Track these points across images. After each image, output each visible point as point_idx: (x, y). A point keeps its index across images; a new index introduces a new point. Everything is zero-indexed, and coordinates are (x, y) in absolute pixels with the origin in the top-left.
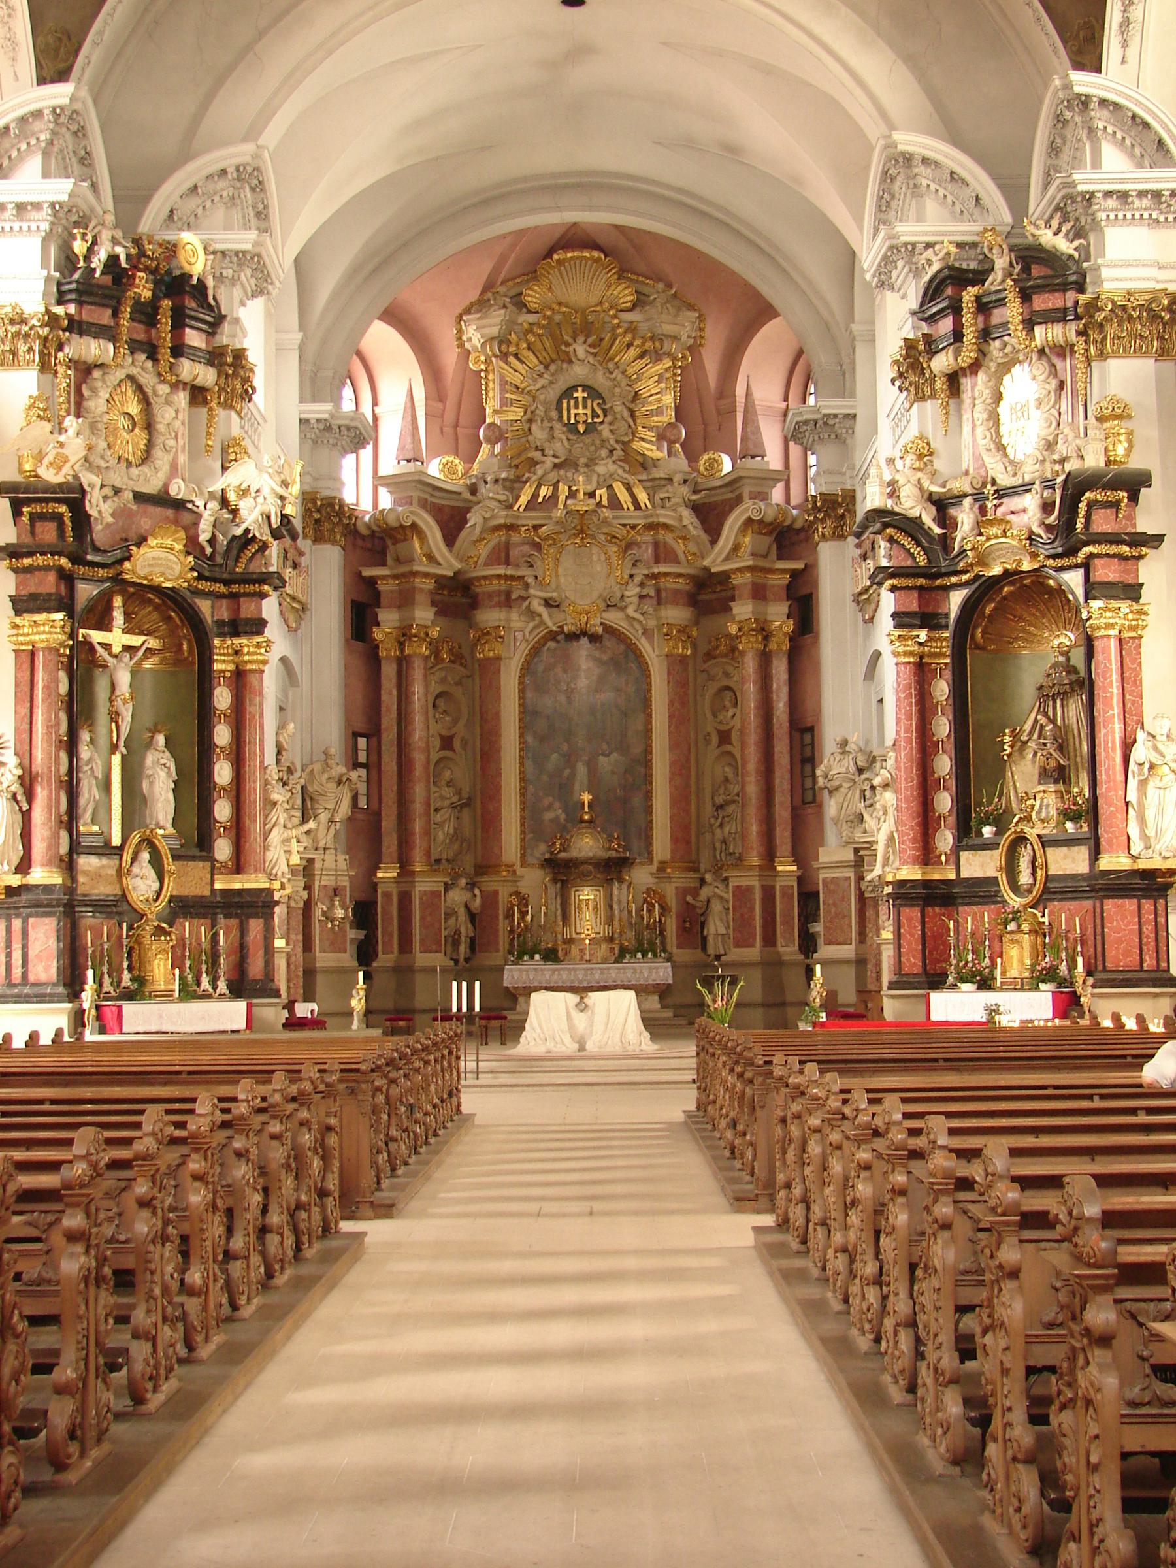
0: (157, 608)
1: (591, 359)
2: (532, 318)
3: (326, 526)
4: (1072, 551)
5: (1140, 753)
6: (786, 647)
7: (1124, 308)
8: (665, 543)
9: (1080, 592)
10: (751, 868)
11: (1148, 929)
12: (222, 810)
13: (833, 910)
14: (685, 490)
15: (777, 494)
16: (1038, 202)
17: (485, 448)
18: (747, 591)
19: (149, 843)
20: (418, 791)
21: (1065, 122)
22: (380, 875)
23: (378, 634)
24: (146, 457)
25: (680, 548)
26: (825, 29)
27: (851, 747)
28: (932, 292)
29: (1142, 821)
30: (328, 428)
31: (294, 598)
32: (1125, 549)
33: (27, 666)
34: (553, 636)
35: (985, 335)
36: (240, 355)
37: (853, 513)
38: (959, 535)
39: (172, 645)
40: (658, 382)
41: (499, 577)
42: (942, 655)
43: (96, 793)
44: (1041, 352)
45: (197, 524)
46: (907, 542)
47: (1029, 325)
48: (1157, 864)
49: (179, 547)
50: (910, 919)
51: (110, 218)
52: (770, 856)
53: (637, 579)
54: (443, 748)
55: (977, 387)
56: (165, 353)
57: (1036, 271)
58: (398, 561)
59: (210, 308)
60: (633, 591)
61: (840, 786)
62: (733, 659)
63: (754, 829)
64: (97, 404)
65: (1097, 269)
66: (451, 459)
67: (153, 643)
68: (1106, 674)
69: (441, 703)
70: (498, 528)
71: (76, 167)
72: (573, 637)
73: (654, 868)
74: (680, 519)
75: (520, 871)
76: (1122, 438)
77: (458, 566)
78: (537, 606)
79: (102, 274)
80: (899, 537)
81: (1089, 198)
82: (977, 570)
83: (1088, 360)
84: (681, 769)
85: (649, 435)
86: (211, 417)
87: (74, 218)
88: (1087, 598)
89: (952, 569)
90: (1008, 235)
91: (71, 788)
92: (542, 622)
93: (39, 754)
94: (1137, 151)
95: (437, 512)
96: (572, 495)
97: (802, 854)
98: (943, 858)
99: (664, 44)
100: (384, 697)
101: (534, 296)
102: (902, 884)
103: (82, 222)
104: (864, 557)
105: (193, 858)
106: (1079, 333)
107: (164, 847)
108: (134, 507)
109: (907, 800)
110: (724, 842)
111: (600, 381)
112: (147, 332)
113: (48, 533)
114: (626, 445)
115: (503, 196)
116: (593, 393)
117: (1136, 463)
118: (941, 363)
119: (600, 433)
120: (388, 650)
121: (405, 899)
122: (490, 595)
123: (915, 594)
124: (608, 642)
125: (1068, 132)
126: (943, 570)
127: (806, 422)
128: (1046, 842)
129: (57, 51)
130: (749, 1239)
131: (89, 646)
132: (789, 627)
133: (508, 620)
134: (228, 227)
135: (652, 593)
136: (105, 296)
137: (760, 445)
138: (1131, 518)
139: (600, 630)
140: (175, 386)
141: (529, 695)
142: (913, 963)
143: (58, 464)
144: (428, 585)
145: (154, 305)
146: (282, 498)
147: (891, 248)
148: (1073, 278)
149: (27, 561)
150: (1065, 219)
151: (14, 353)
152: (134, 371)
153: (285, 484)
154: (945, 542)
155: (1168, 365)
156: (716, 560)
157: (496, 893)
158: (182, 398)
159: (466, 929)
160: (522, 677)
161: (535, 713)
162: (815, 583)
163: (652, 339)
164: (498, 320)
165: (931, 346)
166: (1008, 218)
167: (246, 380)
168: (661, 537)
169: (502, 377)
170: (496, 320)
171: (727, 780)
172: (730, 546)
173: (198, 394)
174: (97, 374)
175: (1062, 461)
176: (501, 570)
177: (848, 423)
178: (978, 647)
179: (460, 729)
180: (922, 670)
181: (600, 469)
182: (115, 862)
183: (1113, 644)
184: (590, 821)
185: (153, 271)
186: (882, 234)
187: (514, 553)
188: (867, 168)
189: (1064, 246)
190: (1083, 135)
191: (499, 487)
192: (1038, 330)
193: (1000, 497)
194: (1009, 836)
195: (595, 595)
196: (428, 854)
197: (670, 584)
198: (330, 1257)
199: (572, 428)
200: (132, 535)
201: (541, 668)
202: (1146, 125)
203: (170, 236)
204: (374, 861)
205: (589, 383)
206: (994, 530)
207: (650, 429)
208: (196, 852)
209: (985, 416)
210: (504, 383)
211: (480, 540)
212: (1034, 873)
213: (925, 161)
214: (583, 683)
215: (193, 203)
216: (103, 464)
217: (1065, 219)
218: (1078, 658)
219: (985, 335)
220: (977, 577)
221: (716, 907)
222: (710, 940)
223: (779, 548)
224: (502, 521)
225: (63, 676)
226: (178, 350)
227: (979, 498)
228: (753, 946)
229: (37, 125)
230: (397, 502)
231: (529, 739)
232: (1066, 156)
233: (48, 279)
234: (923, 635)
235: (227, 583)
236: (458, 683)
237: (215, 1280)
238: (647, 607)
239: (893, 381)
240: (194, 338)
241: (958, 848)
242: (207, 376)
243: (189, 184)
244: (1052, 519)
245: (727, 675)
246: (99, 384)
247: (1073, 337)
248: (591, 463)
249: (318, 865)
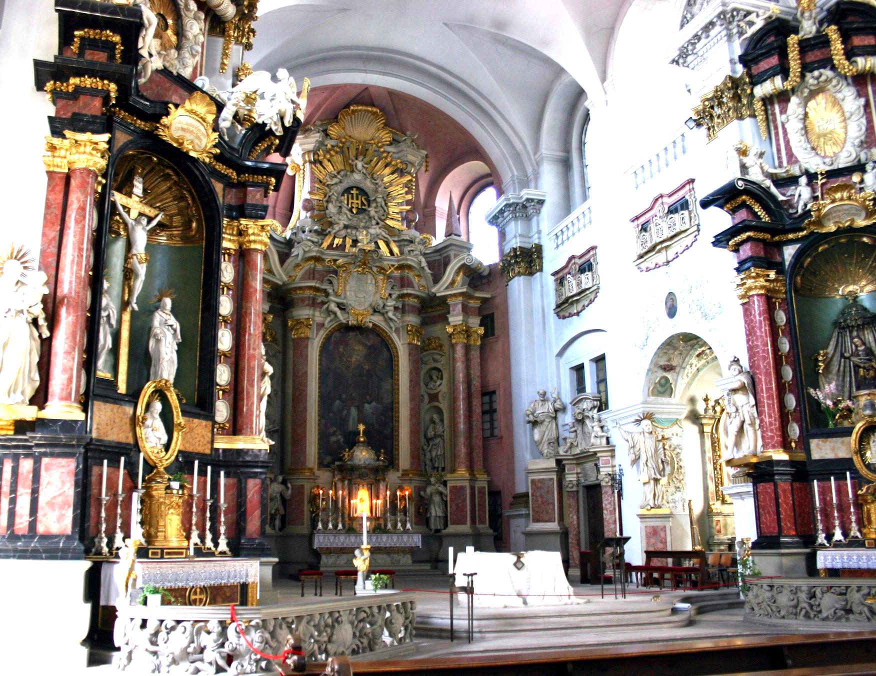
1: (364, 171)
6: (479, 343)
8: (408, 278)
13: (540, 499)
25: (416, 280)
53: (394, 296)
60: (391, 303)
61: (544, 421)
62: (441, 350)
84: (415, 414)
89: (795, 226)
111: (368, 185)
126: (787, 227)
132: (481, 331)
133: (314, 315)
135: (401, 307)
156: (440, 290)
168: (406, 274)
172: (450, 280)
181: (372, 231)
182: (129, 410)
195: (367, 305)
197: (413, 301)
207: (398, 213)
210: (314, 179)
228: (465, 523)
245: (435, 361)
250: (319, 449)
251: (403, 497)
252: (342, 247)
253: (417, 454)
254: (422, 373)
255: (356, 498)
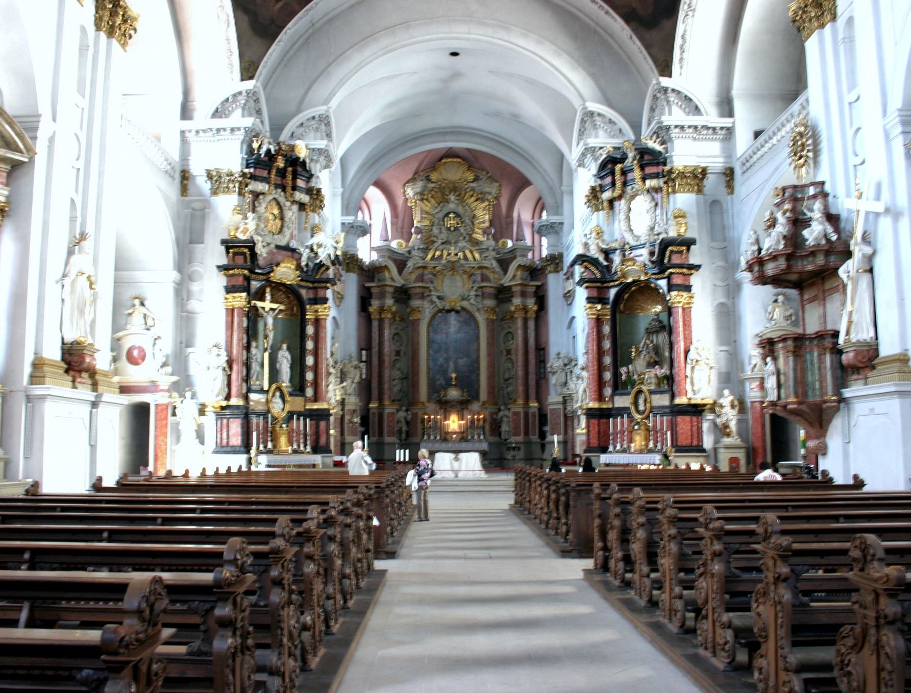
0: (284, 293)
2: (433, 185)
3: (351, 266)
4: (662, 272)
5: (692, 355)
6: (534, 316)
7: (683, 172)
9: (665, 288)
10: (519, 404)
11: (695, 428)
12: (309, 376)
14: (494, 253)
15: (530, 255)
16: (645, 132)
17: (414, 236)
18: (518, 294)
19: (279, 389)
20: (387, 372)
21: (657, 98)
22: (371, 405)
23: (371, 309)
24: (281, 231)
25: (491, 276)
26: (557, 62)
27: (562, 356)
28: (603, 166)
29: (692, 383)
30: (352, 227)
31: (339, 293)
32: (685, 271)
33: (230, 315)
34: (440, 311)
35: (625, 184)
36: (319, 191)
37: (561, 261)
38: (614, 266)
39: (290, 308)
40: (484, 210)
41: (419, 287)
42: (606, 315)
43: (258, 368)
44: (648, 191)
45: (300, 259)
46: (593, 269)
47: (644, 179)
48: (699, 402)
49: (293, 267)
50: (594, 424)
51: (268, 134)
52: (527, 399)
53: (475, 288)
54: (396, 355)
55: (621, 205)
56: (289, 189)
57: (646, 157)
58: (379, 280)
59: (307, 171)
60: (473, 293)
63: (521, 389)
64: (261, 209)
65: (671, 157)
66: (400, 240)
67: (282, 307)
68: (677, 322)
69: (396, 337)
70: (419, 267)
71: (255, 115)
72: (449, 311)
73: (480, 404)
74: (492, 264)
75: (427, 405)
76: (683, 225)
77: (403, 282)
78: (434, 299)
79: (265, 156)
80: (589, 266)
81: (668, 128)
82: (622, 280)
83: (668, 194)
84: (492, 365)
85: (480, 231)
86: (307, 215)
87: (253, 134)
88: (669, 290)
90: (633, 145)
91: (247, 365)
92: (436, 306)
93: (235, 351)
94: (687, 110)
95: (395, 261)
96: (449, 254)
97: (540, 398)
98: (607, 399)
99: (490, 72)
100: (373, 335)
101: (434, 176)
102: (591, 409)
103: (257, 136)
104: (568, 279)
105: (297, 395)
106: (665, 183)
107: (286, 391)
108: (275, 251)
109: (593, 375)
110: (508, 394)
111: (460, 210)
112: (282, 180)
113: (240, 260)
114: (470, 235)
115: (423, 136)
116: (457, 215)
117: (689, 235)
118: (607, 195)
119: (460, 230)
120: (375, 316)
121: (381, 415)
122: (416, 294)
123: (596, 290)
124: (463, 314)
125: (658, 102)
127: (543, 226)
128: (651, 392)
129: (249, 69)
130: (581, 575)
131: (255, 308)
132: (535, 308)
133: (423, 304)
134: (315, 139)
136: (265, 165)
137: (524, 236)
138: (687, 258)
139: (459, 308)
140: (294, 202)
141: (431, 334)
142: (594, 442)
143: (245, 231)
144: (391, 290)
145: (285, 169)
146: (336, 248)
147: (585, 149)
148: (662, 160)
149: (231, 272)
150: (658, 137)
151: (228, 187)
152: (276, 196)
153: (337, 242)
154: (608, 268)
155: (701, 196)
156: (506, 281)
157: (417, 413)
158: (295, 208)
159: (404, 428)
160: (428, 327)
161: (433, 342)
162: (546, 291)
163: (481, 193)
164: (420, 186)
165: (602, 189)
166: (632, 137)
167: (322, 201)
169: (421, 208)
170: (419, 186)
171: (509, 369)
172: (512, 275)
173: (302, 206)
174: (261, 197)
175: (659, 234)
176: (420, 284)
177: (560, 226)
178: (622, 312)
179: (403, 349)
180: (598, 321)
183: (680, 311)
184: (455, 385)
185: (285, 156)
186: (582, 143)
187: (425, 277)
188: (573, 121)
189: (658, 147)
190: (665, 103)
191: (419, 251)
192: (648, 182)
193: (632, 250)
194: (635, 390)
195: (457, 295)
196: (390, 397)
197: (487, 290)
198: (373, 590)
199: (449, 229)
200: (274, 262)
201: (436, 323)
202: (690, 100)
203: (292, 143)
204: (368, 400)
205: (456, 211)
206: (629, 263)
207: (480, 229)
208: (298, 393)
209: (624, 217)
210: (422, 211)
211: (412, 273)
212: (645, 405)
213: (599, 115)
214: (452, 330)
215: (301, 130)
216: (263, 233)
217: (658, 137)
218: (664, 317)
219: (625, 184)
220: (622, 283)
221: (505, 419)
222: (503, 433)
223: (531, 277)
224: (420, 265)
225: (245, 319)
226: (294, 188)
227: (623, 251)
228: (519, 435)
229: (240, 97)
230: (380, 257)
231: (431, 352)
232: (657, 112)
233: (243, 158)
234: (599, 307)
235: (313, 282)
236: (403, 330)
237: (319, 617)
238: (479, 299)
239: (586, 203)
240: (301, 183)
241: (614, 394)
242: (305, 198)
243: (300, 122)
244: (654, 258)
245: (509, 327)
246: (262, 201)
247: (662, 184)
248: (456, 242)
249: (346, 401)
250: (428, 389)
251: (478, 420)
252: (441, 256)
253: (492, 391)
254: (502, 335)
255: (449, 420)
